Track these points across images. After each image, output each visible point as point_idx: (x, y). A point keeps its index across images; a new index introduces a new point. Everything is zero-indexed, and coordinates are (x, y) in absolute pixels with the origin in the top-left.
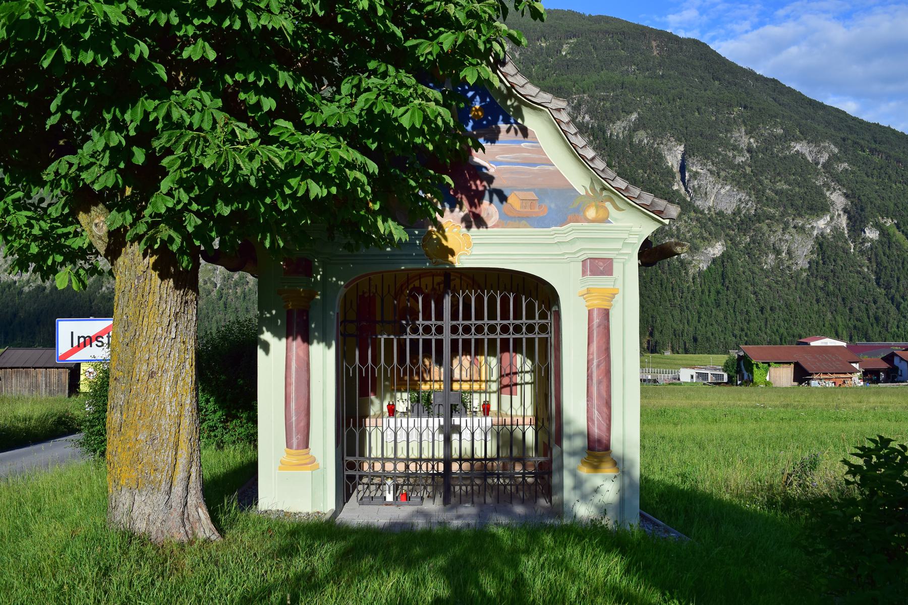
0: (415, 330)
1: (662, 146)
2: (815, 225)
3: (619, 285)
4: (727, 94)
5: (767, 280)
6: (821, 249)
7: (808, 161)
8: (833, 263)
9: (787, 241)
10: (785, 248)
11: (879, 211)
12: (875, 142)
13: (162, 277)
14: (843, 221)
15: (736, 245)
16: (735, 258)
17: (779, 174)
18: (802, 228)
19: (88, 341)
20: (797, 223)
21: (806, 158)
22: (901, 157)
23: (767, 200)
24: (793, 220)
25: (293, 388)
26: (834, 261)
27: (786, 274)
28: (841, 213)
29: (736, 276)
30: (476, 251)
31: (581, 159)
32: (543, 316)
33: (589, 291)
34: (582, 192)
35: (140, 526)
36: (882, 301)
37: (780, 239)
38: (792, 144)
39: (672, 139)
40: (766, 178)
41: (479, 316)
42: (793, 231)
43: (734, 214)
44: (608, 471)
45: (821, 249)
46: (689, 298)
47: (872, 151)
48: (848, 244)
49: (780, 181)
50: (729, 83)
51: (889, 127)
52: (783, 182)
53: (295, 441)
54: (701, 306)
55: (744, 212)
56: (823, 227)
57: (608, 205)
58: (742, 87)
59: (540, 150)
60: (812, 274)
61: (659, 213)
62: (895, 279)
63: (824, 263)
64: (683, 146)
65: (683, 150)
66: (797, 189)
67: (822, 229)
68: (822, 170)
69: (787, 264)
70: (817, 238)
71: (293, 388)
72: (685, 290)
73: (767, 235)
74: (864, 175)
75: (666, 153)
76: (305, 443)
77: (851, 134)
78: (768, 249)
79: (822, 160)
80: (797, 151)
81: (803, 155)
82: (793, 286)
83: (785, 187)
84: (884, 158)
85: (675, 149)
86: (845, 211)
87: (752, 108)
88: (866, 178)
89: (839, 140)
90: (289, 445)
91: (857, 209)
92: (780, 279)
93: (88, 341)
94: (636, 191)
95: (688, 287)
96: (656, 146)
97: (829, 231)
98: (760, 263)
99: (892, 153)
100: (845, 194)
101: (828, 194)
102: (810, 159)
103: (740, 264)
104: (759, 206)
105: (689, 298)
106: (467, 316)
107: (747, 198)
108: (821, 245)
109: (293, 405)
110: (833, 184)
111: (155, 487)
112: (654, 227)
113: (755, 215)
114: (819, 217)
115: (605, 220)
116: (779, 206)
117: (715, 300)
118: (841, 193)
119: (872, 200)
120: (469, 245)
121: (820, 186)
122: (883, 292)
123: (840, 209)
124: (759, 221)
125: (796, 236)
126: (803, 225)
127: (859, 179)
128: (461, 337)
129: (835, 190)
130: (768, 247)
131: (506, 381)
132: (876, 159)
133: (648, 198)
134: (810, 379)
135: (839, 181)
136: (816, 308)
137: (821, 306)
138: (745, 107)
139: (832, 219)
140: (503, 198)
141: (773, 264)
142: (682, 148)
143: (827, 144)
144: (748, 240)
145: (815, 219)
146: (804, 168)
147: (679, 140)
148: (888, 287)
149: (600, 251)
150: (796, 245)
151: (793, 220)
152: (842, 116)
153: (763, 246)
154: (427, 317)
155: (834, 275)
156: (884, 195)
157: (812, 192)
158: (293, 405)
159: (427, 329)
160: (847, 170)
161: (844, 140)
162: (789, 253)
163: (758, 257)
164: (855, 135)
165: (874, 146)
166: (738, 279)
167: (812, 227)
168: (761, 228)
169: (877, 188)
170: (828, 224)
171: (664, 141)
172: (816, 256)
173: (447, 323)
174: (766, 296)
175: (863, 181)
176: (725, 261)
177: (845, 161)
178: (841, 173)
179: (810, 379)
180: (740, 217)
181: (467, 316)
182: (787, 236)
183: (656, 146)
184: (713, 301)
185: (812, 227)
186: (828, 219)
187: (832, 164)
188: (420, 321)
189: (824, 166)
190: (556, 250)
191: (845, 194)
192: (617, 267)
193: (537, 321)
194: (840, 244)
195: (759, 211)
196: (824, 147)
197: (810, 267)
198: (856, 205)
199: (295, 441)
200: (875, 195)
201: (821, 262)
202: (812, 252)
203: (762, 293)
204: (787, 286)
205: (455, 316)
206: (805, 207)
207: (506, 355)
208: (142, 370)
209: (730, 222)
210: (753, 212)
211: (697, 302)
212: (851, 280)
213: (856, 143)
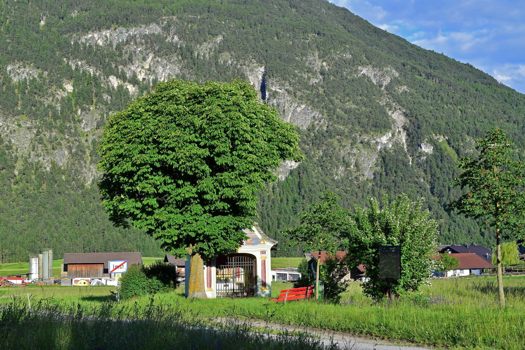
1: (244, 67)
2: (379, 140)
4: (302, 21)
5: (337, 190)
6: (384, 161)
7: (373, 83)
8: (395, 175)
9: (355, 155)
10: (353, 161)
11: (433, 129)
12: (430, 67)
14: (403, 137)
15: (311, 158)
16: (309, 170)
17: (348, 95)
18: (368, 143)
19: (118, 267)
20: (364, 139)
21: (371, 81)
22: (452, 81)
23: (337, 118)
24: (360, 136)
26: (395, 172)
27: (354, 184)
28: (401, 130)
29: (310, 186)
31: (260, 233)
32: (252, 261)
35: (199, 297)
36: (436, 208)
37: (349, 153)
38: (360, 68)
39: (254, 61)
40: (337, 98)
41: (240, 261)
42: (360, 146)
43: (309, 130)
45: (384, 161)
46: (269, 206)
47: (428, 76)
48: (407, 158)
49: (349, 101)
50: (304, 11)
51: (442, 54)
52: (351, 102)
54: (280, 213)
55: (317, 128)
56: (386, 142)
58: (316, 15)
60: (377, 184)
62: (447, 189)
63: (386, 175)
64: (263, 67)
65: (263, 71)
66: (363, 109)
67: (385, 144)
68: (385, 92)
69: (355, 175)
70: (380, 152)
72: (266, 199)
73: (337, 149)
74: (421, 97)
75: (248, 73)
76: (210, 286)
77: (410, 59)
78: (339, 162)
79: (385, 83)
80: (364, 75)
81: (369, 78)
82: (360, 195)
83: (353, 106)
84: (438, 82)
85: (257, 70)
86: (405, 128)
87: (324, 35)
88: (422, 100)
89: (399, 65)
90: (208, 287)
91: (414, 126)
92: (349, 189)
93: (118, 267)
95: (269, 196)
96: (239, 66)
97: (390, 146)
98: (332, 175)
99: (445, 78)
100: (404, 113)
101: (390, 113)
102: (374, 82)
103: (314, 175)
104: (330, 123)
105: (269, 206)
106: (237, 261)
107: (320, 116)
108: (384, 158)
110: (394, 104)
111: (201, 291)
112: (273, 245)
113: (327, 132)
114: (382, 134)
116: (348, 123)
117: (293, 208)
118: (400, 112)
119: (427, 119)
121: (383, 106)
122: (437, 199)
123: (400, 127)
124: (330, 137)
125: (363, 151)
126: (369, 140)
127: (416, 101)
129: (396, 109)
130: (338, 160)
131: (237, 274)
132: (431, 82)
134: (362, 276)
135: (399, 102)
138: (319, 34)
139: (393, 135)
141: (343, 175)
142: (262, 69)
143: (389, 69)
144: (321, 153)
145: (379, 135)
146: (370, 90)
147: (260, 62)
148: (440, 196)
150: (363, 158)
151: (360, 136)
152: (402, 43)
153: (334, 159)
154: (230, 262)
155: (395, 185)
156: (437, 115)
157: (377, 111)
159: (230, 264)
160: (406, 92)
161: (404, 65)
162: (356, 165)
163: (330, 169)
164: (414, 61)
165: (429, 71)
166: (313, 189)
167: (376, 142)
168: (333, 143)
169: (432, 108)
170: (390, 140)
171: (247, 63)
172: (379, 168)
173: (233, 263)
175: (419, 102)
176: (301, 172)
177: (405, 84)
178: (401, 95)
179: (362, 276)
180: (314, 133)
181: (237, 261)
182: (355, 151)
183: (239, 66)
184: (291, 209)
185: (376, 142)
186: (390, 135)
187: (393, 87)
189: (386, 88)
191: (404, 113)
192: (267, 252)
193: (251, 262)
194: (400, 157)
195: (330, 128)
196: (387, 72)
197: (375, 178)
198: (413, 124)
200: (430, 114)
201: (384, 173)
202: (376, 165)
204: (355, 195)
205: (235, 262)
206: (370, 125)
209: (305, 137)
210: (325, 128)
211: (276, 210)
212: (410, 189)
213: (413, 68)
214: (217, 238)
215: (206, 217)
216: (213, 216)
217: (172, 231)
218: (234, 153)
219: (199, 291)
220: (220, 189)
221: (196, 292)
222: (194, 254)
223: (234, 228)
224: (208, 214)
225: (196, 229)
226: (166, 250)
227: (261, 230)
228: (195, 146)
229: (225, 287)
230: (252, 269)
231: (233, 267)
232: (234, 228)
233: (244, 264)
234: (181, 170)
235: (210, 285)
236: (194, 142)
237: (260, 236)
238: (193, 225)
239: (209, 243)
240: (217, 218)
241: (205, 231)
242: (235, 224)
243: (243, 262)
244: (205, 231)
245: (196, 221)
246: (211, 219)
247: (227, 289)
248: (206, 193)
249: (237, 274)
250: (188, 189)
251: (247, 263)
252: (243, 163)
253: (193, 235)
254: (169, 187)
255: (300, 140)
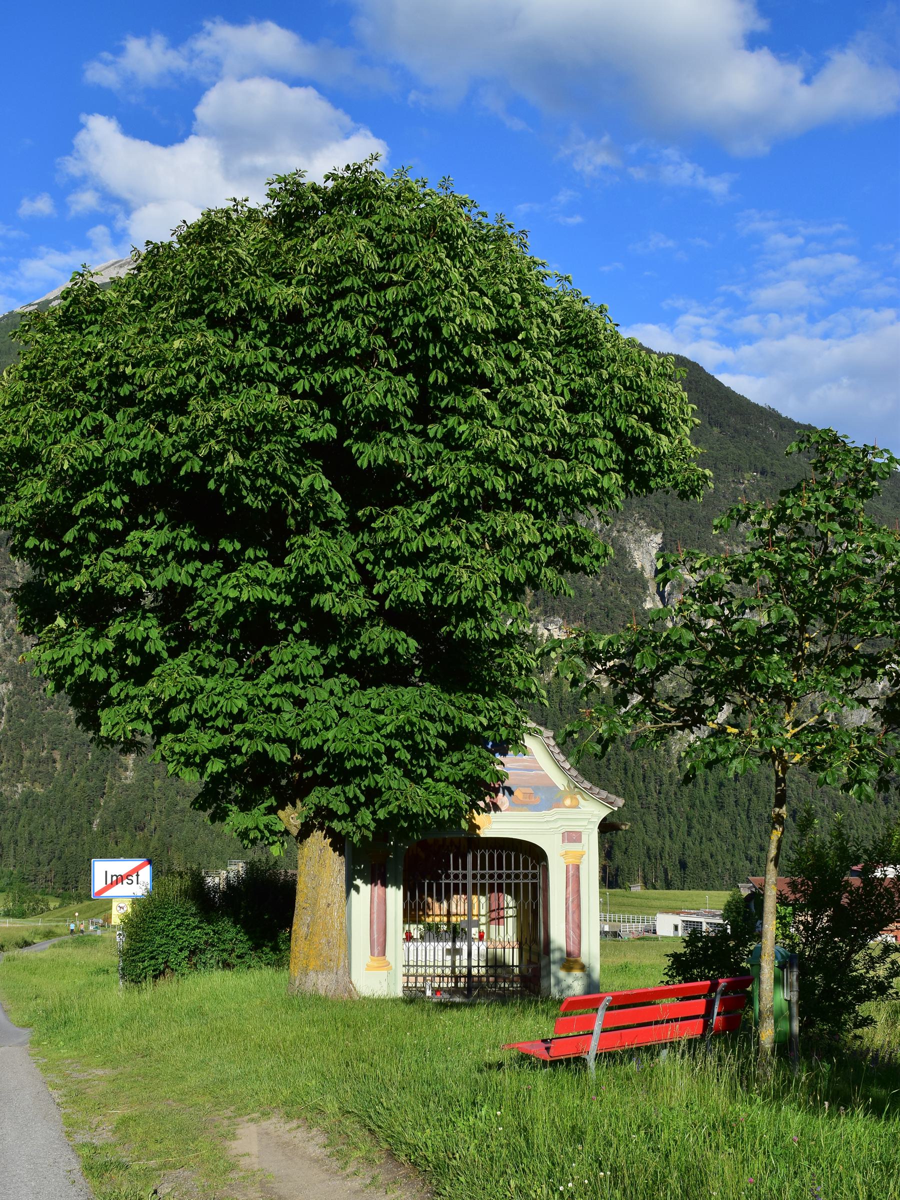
0: (448, 877)
3: (586, 849)
13: (334, 851)
25: (375, 916)
30: (494, 826)
31: (562, 769)
32: (534, 868)
33: (566, 853)
34: (562, 788)
44: (577, 973)
46: (672, 793)
53: (376, 952)
54: (692, 806)
57: (578, 796)
59: (535, 761)
61: (611, 803)
71: (375, 916)
72: (666, 779)
76: (383, 953)
90: (372, 954)
94: (597, 790)
95: (671, 776)
105: (672, 793)
106: (483, 868)
109: (375, 927)
111: (330, 970)
115: (577, 807)
117: (716, 797)
120: (490, 823)
128: (479, 882)
131: (494, 915)
133: (604, 794)
136: (883, 812)
137: (892, 809)
140: (511, 792)
149: (573, 827)
158: (375, 927)
159: (456, 877)
173: (470, 872)
174: (801, 791)
181: (483, 868)
184: (712, 799)
188: (452, 871)
190: (546, 826)
192: (584, 838)
193: (530, 871)
199: (376, 952)
203: (793, 786)
205: (474, 867)
207: (494, 895)
208: (323, 903)
211: (685, 800)
214: (377, 770)
215: (338, 690)
216: (363, 687)
217: (207, 738)
218: (433, 430)
219: (324, 968)
220: (379, 572)
221: (312, 975)
222: (305, 832)
223: (442, 735)
224: (344, 677)
225: (292, 734)
226: (213, 818)
227: (561, 758)
228: (269, 391)
229: (449, 958)
230: (535, 897)
231: (469, 888)
232: (442, 735)
233: (509, 876)
234: (218, 487)
235: (379, 946)
236: (269, 378)
237: (559, 780)
238: (286, 716)
239: (347, 789)
240: (374, 696)
241: (325, 741)
242: (448, 720)
243: (513, 871)
244: (325, 741)
245: (300, 703)
246: (354, 698)
247: (457, 964)
248: (316, 585)
249: (494, 915)
250: (255, 572)
251: (522, 874)
252: (462, 464)
253: (281, 753)
254: (191, 568)
255: (697, 421)
